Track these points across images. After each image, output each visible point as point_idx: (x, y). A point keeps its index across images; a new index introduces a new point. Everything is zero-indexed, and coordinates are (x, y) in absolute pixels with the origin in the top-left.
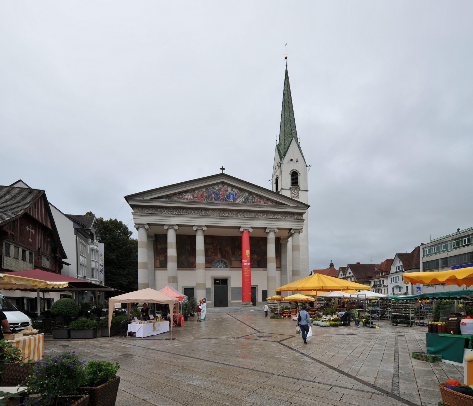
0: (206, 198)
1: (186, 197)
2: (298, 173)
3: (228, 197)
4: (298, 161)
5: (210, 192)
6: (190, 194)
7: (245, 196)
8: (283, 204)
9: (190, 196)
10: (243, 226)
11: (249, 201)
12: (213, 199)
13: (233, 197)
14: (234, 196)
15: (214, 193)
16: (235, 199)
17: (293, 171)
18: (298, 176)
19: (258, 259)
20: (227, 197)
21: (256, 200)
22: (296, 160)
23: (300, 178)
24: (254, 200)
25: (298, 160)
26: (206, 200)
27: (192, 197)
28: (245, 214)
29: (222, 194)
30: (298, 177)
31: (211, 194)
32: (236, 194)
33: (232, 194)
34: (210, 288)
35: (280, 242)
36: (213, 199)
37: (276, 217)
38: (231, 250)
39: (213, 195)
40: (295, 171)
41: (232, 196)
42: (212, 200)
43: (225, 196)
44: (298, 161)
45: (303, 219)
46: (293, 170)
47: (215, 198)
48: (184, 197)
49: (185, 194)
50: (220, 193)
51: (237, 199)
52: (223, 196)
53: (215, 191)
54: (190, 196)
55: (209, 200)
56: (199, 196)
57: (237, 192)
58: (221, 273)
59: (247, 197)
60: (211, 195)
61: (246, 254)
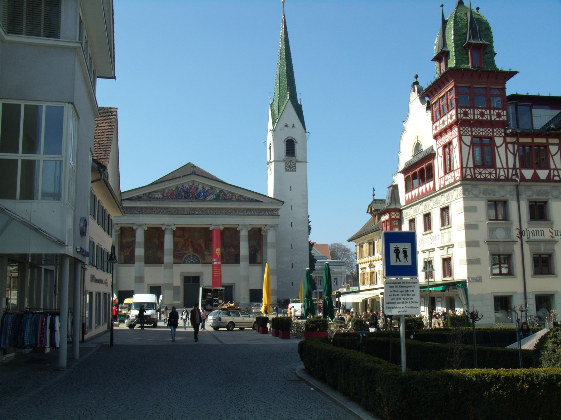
0: (176, 196)
1: (156, 196)
2: (295, 141)
3: (199, 195)
4: (294, 127)
5: (180, 190)
6: (159, 193)
7: (216, 193)
8: (257, 201)
9: (159, 195)
11: (220, 198)
12: (183, 197)
13: (204, 194)
14: (205, 194)
15: (184, 191)
16: (205, 197)
17: (288, 139)
18: (294, 145)
19: (235, 253)
20: (197, 195)
21: (227, 197)
22: (292, 126)
23: (297, 147)
24: (226, 196)
25: (295, 126)
26: (176, 198)
27: (161, 196)
29: (192, 192)
30: (294, 146)
31: (181, 193)
33: (203, 192)
34: (179, 287)
35: (262, 233)
36: (183, 197)
37: (248, 213)
38: (204, 243)
39: (183, 193)
40: (290, 138)
41: (202, 194)
42: (182, 198)
43: (196, 194)
44: (294, 127)
45: (278, 215)
46: (288, 138)
48: (154, 197)
49: (155, 194)
50: (191, 191)
51: (208, 196)
52: (193, 193)
53: (185, 189)
54: (159, 195)
55: (179, 199)
56: (169, 195)
57: (208, 189)
58: (192, 269)
59: (218, 194)
60: (181, 194)
61: (217, 253)
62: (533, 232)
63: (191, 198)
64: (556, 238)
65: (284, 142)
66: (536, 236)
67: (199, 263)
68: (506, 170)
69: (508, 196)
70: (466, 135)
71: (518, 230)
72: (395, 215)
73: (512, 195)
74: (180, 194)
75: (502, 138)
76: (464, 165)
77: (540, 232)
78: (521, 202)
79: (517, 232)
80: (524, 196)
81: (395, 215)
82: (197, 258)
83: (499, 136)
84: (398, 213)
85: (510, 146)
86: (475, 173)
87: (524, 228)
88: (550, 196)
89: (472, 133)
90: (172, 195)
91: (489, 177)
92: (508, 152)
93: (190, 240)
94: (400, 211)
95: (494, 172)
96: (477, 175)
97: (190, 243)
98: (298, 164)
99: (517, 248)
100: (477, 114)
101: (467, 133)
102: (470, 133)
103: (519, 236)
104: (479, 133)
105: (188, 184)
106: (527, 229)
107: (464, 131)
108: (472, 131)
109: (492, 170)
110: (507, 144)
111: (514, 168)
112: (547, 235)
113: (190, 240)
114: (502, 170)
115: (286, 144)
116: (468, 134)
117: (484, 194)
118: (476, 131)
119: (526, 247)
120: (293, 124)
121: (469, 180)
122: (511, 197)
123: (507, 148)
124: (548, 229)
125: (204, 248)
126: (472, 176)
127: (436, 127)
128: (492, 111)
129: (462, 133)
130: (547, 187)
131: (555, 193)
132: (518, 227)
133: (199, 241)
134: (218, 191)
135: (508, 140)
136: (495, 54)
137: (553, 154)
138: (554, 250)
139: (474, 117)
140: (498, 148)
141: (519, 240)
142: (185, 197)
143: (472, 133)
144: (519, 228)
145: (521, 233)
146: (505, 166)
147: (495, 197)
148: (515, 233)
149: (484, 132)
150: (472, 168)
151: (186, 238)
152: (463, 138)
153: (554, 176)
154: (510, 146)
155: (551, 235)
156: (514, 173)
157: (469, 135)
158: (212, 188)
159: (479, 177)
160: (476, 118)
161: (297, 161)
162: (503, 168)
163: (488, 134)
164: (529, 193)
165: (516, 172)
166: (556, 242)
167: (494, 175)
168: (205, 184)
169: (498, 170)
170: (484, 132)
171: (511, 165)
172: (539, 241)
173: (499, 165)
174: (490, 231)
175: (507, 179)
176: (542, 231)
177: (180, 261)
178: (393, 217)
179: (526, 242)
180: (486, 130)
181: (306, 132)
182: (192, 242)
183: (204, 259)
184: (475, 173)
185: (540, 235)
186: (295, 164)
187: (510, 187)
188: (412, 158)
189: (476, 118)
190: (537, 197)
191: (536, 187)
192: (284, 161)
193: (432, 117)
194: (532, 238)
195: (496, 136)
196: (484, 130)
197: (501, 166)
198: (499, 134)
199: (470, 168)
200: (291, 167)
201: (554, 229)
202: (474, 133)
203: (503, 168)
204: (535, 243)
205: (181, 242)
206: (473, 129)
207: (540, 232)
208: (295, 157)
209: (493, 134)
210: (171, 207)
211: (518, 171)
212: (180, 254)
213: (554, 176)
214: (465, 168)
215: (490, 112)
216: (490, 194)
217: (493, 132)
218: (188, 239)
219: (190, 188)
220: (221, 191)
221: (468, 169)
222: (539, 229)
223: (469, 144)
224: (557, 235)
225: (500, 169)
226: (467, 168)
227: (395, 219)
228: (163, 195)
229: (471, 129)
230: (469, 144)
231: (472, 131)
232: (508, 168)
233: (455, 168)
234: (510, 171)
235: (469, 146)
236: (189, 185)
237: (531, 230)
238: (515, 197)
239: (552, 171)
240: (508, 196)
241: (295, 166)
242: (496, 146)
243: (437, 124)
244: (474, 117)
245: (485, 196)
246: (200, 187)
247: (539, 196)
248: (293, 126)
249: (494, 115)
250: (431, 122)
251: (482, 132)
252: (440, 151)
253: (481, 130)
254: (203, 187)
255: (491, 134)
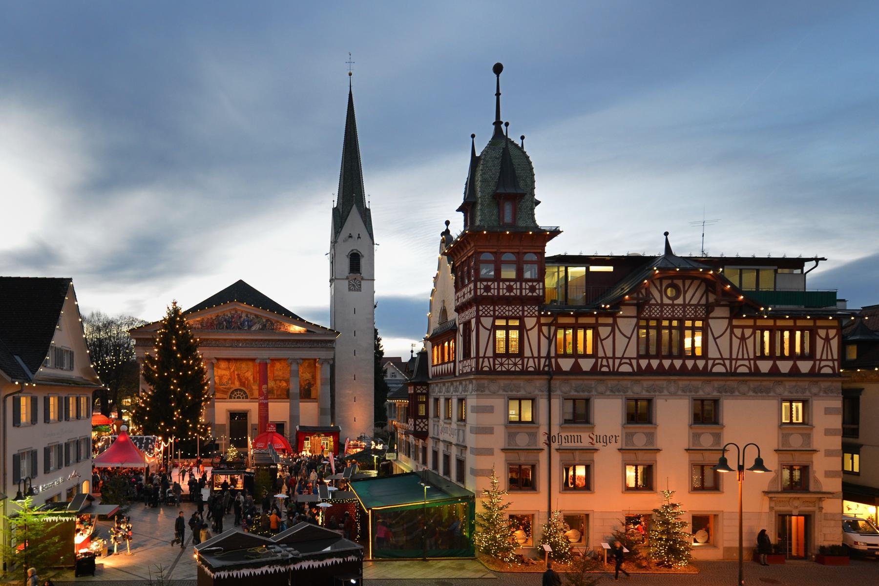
3: (242, 324)
10: (258, 357)
15: (225, 320)
16: (250, 327)
18: (359, 259)
20: (241, 324)
23: (363, 262)
27: (200, 326)
28: (262, 343)
31: (223, 322)
32: (251, 321)
33: (247, 321)
37: (299, 345)
39: (225, 323)
40: (355, 251)
41: (246, 323)
42: (223, 328)
46: (352, 250)
47: (226, 327)
51: (253, 326)
52: (236, 323)
62: (566, 437)
63: (233, 328)
64: (597, 446)
65: (348, 256)
66: (570, 443)
67: (247, 398)
68: (536, 360)
69: (537, 392)
70: (486, 316)
71: (547, 436)
72: (422, 389)
73: (542, 391)
74: (220, 323)
75: (536, 319)
76: (481, 355)
77: (576, 437)
78: (553, 401)
79: (546, 437)
80: (558, 392)
81: (422, 389)
82: (245, 393)
83: (531, 316)
84: (424, 387)
85: (545, 329)
86: (494, 364)
87: (555, 431)
88: (594, 393)
89: (494, 313)
90: (212, 324)
91: (513, 369)
92: (542, 337)
93: (236, 373)
94: (428, 385)
95: (520, 362)
96: (497, 366)
97: (236, 376)
98: (363, 282)
99: (543, 457)
100: (503, 289)
101: (489, 313)
102: (492, 313)
103: (547, 442)
104: (504, 313)
105: (230, 312)
106: (558, 434)
107: (484, 310)
108: (494, 311)
109: (517, 360)
110: (540, 325)
111: (548, 357)
112: (586, 442)
113: (236, 373)
114: (531, 360)
115: (350, 258)
116: (489, 315)
117: (504, 390)
118: (500, 311)
119: (556, 458)
120: (359, 234)
121: (486, 373)
122: (540, 393)
123: (540, 331)
124: (588, 434)
125: (252, 382)
126: (490, 368)
127: (458, 298)
128: (524, 284)
129: (481, 313)
130: (591, 382)
131: (601, 388)
132: (548, 433)
133: (246, 374)
134: (264, 320)
135: (543, 320)
136: (538, 203)
137: (602, 337)
138: (593, 461)
139: (498, 292)
140: (529, 332)
141: (546, 447)
142: (226, 327)
143: (494, 313)
144: (548, 433)
145: (550, 439)
146: (536, 355)
147: (519, 393)
148: (542, 439)
149: (511, 311)
150: (491, 357)
151: (232, 370)
152: (482, 319)
153: (602, 366)
154: (545, 329)
155: (591, 441)
156: (547, 363)
157: (491, 316)
158: (257, 316)
159: (499, 369)
160: (501, 294)
161: (362, 279)
162: (533, 357)
163: (516, 313)
164: (566, 388)
165: (550, 362)
166: (597, 450)
167: (520, 367)
168: (249, 312)
169: (526, 360)
170: (511, 311)
171: (544, 353)
172: (573, 450)
173: (527, 353)
174: (509, 436)
175: (537, 372)
176: (579, 437)
177: (225, 396)
178: (419, 391)
179: (557, 450)
180: (513, 308)
181: (373, 244)
182: (238, 375)
183: (252, 394)
184: (494, 364)
185: (576, 441)
186: (360, 282)
187: (540, 382)
188: (438, 326)
189: (501, 294)
190: (576, 393)
191: (576, 382)
192: (347, 278)
193: (456, 282)
194: (565, 445)
195: (527, 316)
196: (511, 308)
197: (530, 355)
198: (531, 313)
199: (488, 358)
200: (355, 287)
201: (595, 434)
202: (497, 313)
203: (533, 357)
204: (568, 451)
205: (227, 375)
206: (497, 308)
207: (576, 437)
208: (361, 274)
209: (523, 313)
210: (211, 339)
211: (553, 360)
212: (225, 388)
213: (602, 366)
214: (481, 357)
215: (521, 285)
216: (512, 391)
217: (523, 311)
218: (234, 371)
219: (233, 317)
220: (268, 320)
221: (486, 360)
222: (575, 434)
223: (490, 328)
224: (598, 441)
225: (528, 358)
226: (484, 357)
227: (422, 394)
228: (202, 325)
229: (494, 308)
230: (490, 328)
231: (494, 311)
232: (539, 357)
233: (472, 356)
234: (543, 361)
235: (490, 330)
236: (231, 314)
237: (564, 435)
238: (546, 393)
239: (600, 360)
240: (537, 392)
241: (360, 285)
242: (526, 328)
243: (460, 294)
244: (498, 292)
245: (505, 393)
246: (244, 315)
247: (578, 392)
248: (359, 237)
249: (526, 289)
250: (454, 290)
251: (509, 311)
252: (461, 327)
253: (507, 308)
254: (247, 316)
255: (521, 313)
